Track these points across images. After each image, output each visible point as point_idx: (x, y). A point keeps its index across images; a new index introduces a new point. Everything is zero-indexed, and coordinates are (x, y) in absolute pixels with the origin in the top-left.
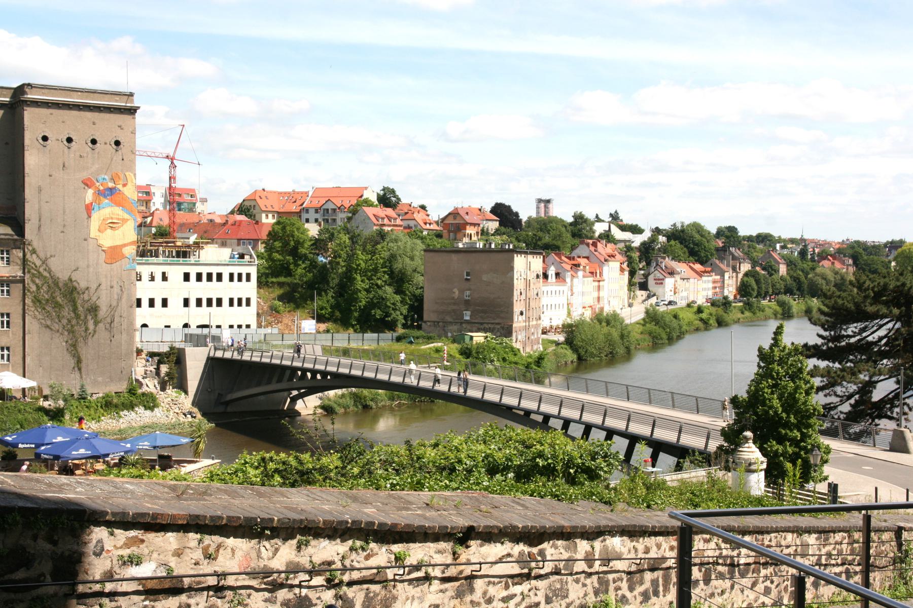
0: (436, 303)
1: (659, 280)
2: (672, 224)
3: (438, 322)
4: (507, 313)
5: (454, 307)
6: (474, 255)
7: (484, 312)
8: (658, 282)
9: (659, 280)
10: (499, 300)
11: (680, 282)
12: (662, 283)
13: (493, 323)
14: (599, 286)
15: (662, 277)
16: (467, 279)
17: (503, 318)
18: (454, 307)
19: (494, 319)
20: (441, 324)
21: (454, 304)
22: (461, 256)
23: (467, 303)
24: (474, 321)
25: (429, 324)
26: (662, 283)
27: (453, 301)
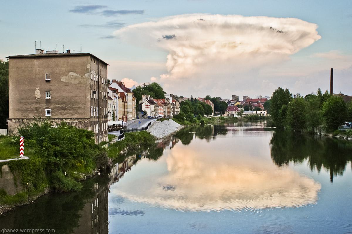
0: (21, 103)
1: (147, 106)
2: (143, 84)
3: (22, 119)
4: (84, 109)
5: (38, 106)
6: (53, 60)
7: (64, 109)
8: (147, 107)
9: (147, 106)
10: (77, 98)
11: (156, 108)
12: (149, 108)
13: (71, 119)
14: (125, 105)
15: (149, 104)
16: (47, 81)
17: (80, 114)
18: (38, 106)
19: (73, 115)
20: (25, 120)
21: (37, 103)
22: (42, 61)
23: (48, 101)
24: (54, 117)
25: (14, 121)
26: (149, 108)
27: (35, 100)
